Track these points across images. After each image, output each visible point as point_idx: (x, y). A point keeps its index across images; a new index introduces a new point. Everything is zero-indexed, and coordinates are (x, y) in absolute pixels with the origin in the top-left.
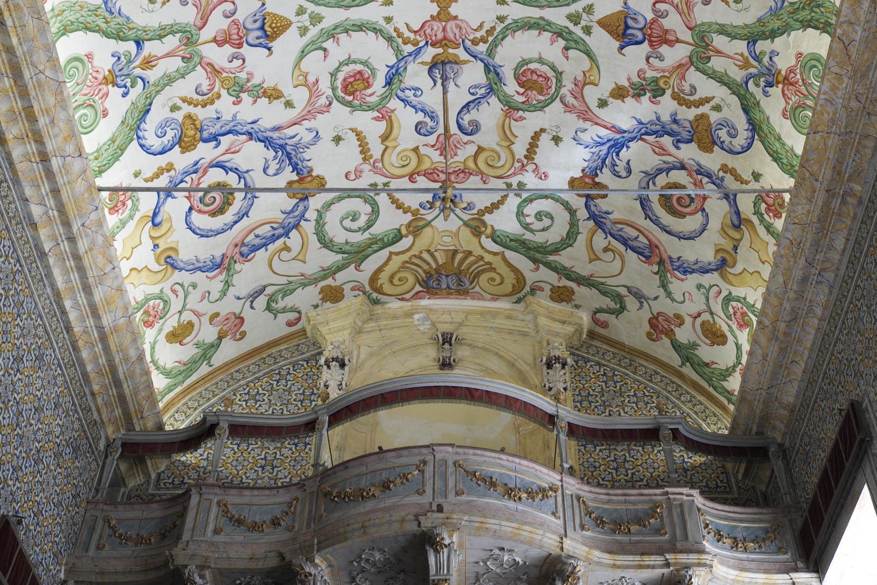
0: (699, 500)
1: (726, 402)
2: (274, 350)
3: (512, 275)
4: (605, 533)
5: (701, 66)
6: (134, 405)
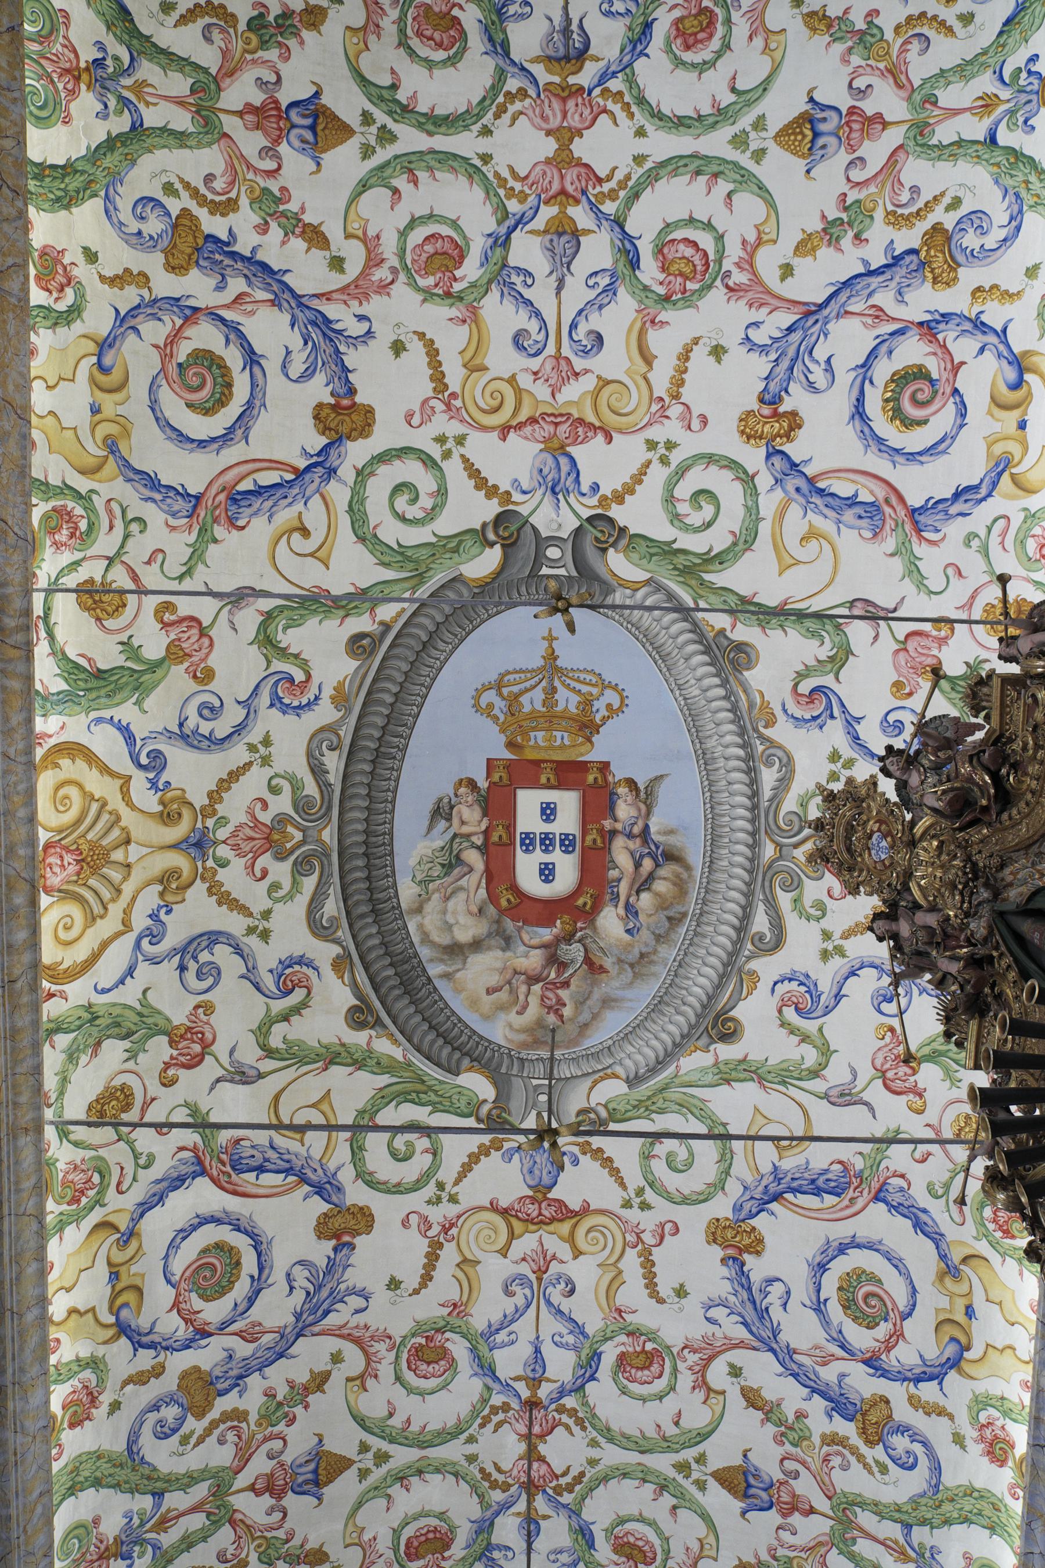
5: (202, 77)
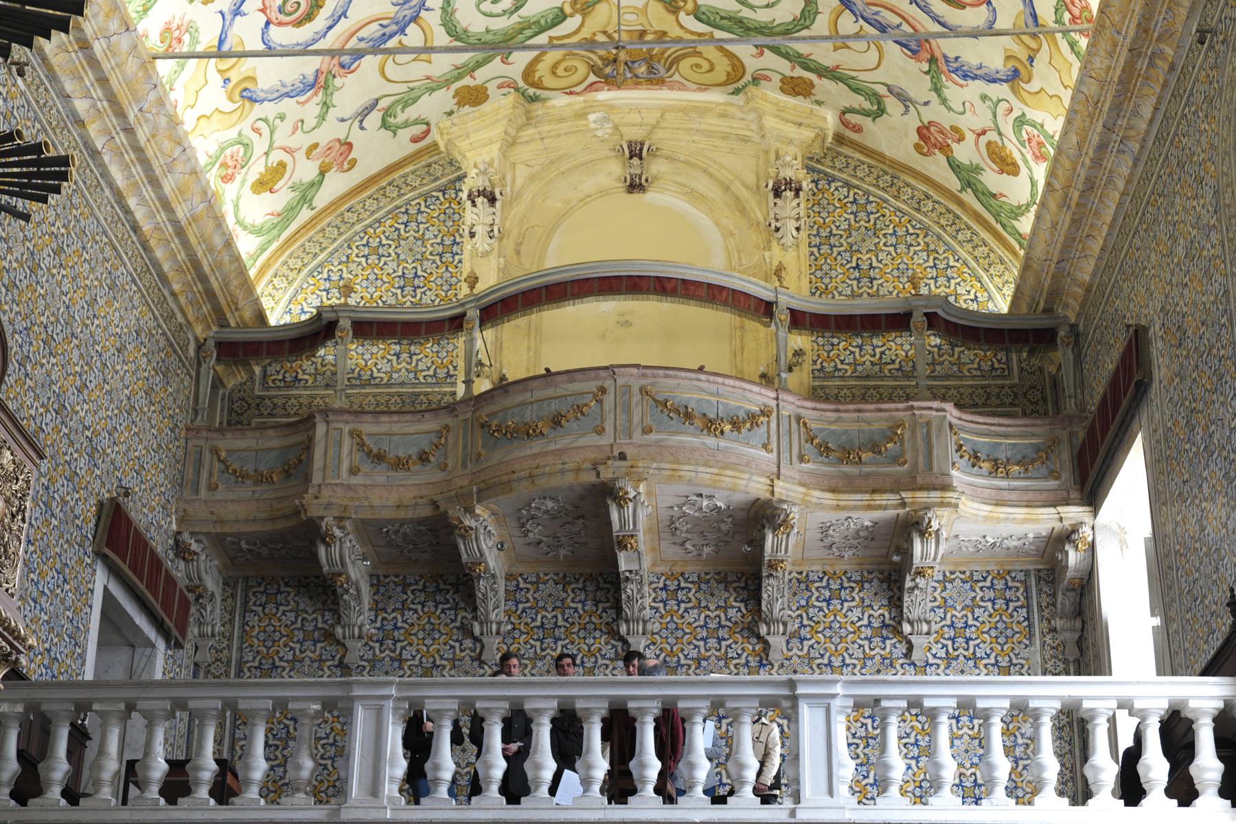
0: (952, 413)
1: (1017, 247)
2: (396, 175)
3: (725, 61)
4: (829, 464)
6: (225, 297)
